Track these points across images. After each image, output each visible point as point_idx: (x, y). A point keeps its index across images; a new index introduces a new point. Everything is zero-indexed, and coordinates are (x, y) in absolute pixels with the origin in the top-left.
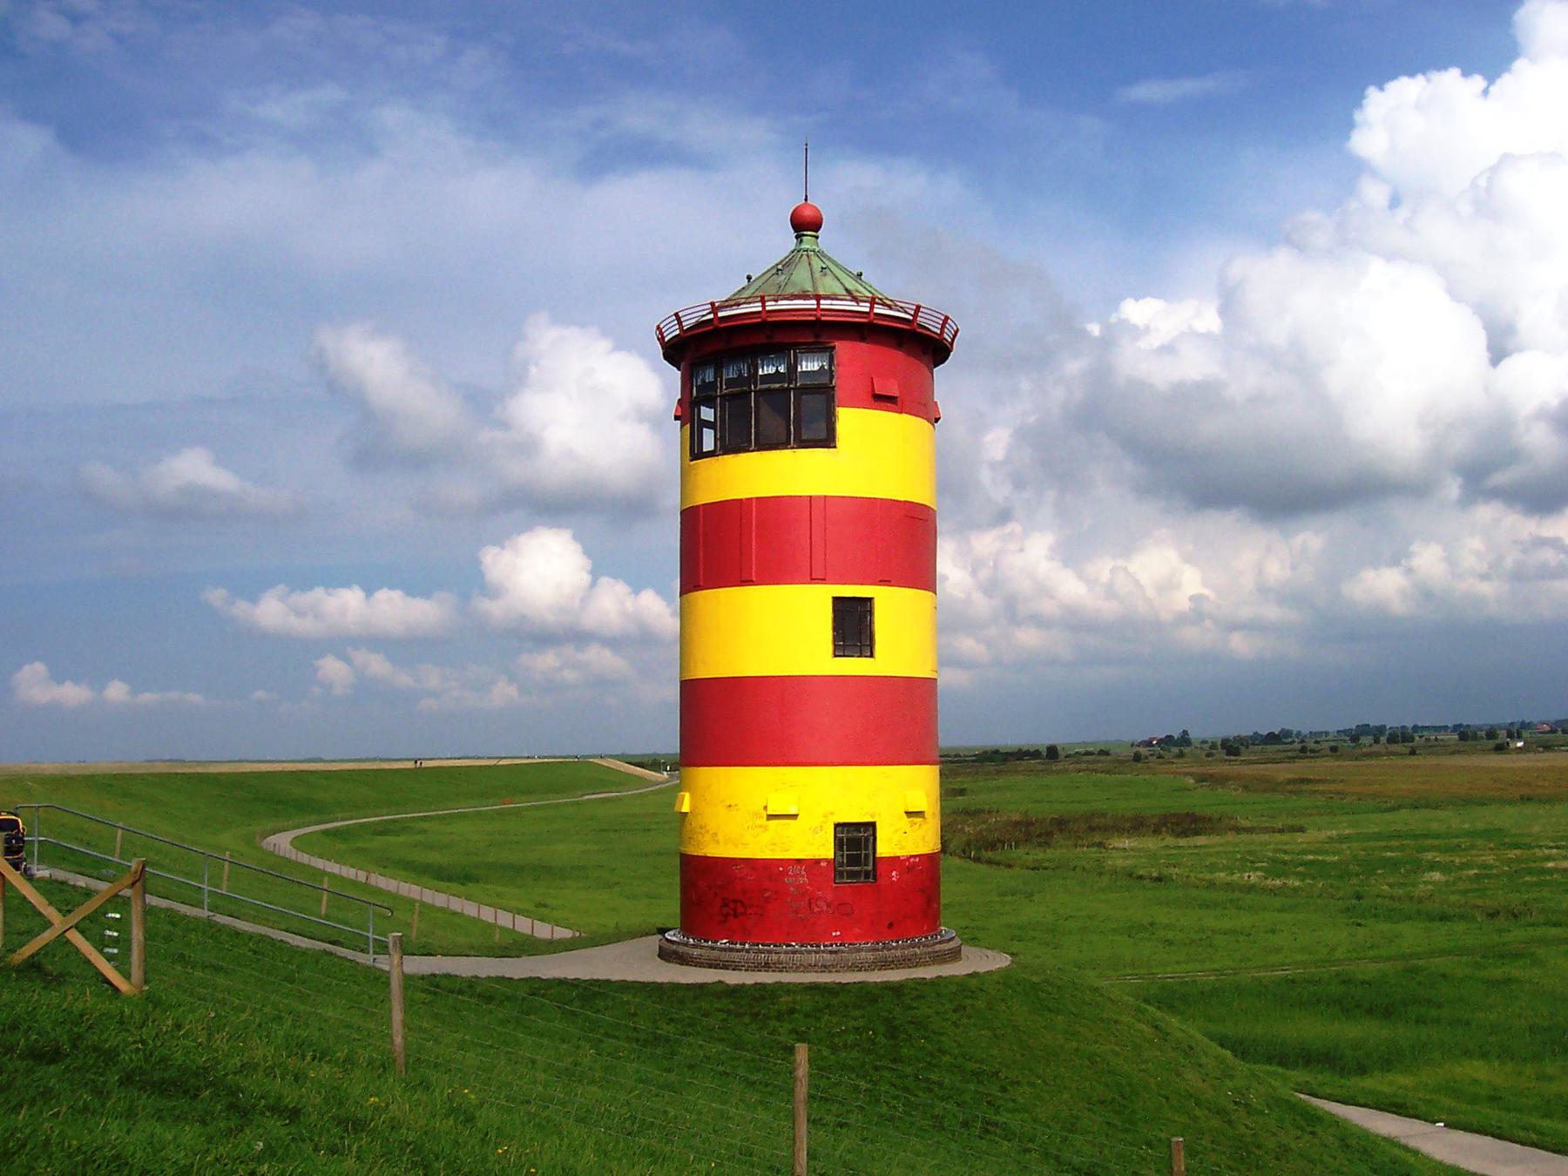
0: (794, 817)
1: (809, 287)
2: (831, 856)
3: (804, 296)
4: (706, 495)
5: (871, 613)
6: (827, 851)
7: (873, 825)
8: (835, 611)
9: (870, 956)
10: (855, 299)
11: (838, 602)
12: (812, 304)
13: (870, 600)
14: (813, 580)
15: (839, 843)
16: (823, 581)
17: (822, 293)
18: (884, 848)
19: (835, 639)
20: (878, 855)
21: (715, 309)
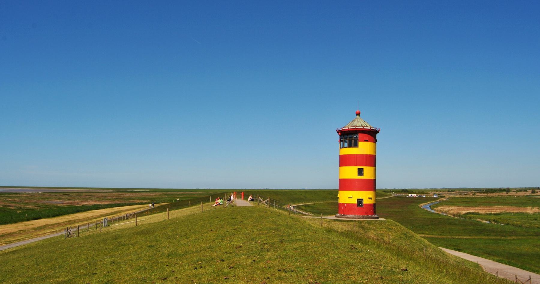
0: (352, 198)
1: (356, 125)
2: (357, 203)
3: (355, 126)
4: (342, 154)
5: (363, 170)
6: (356, 202)
7: (363, 199)
8: (358, 170)
9: (361, 217)
10: (362, 126)
11: (358, 169)
12: (355, 128)
13: (363, 169)
14: (355, 166)
15: (358, 202)
16: (356, 166)
17: (357, 126)
18: (365, 202)
19: (358, 174)
20: (364, 203)
21: (342, 128)
